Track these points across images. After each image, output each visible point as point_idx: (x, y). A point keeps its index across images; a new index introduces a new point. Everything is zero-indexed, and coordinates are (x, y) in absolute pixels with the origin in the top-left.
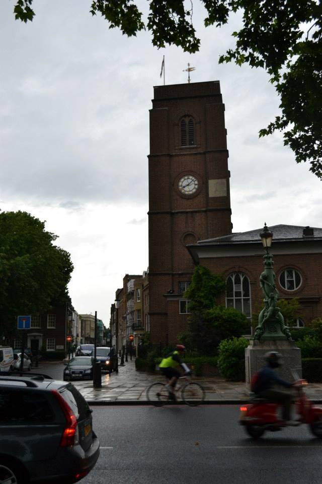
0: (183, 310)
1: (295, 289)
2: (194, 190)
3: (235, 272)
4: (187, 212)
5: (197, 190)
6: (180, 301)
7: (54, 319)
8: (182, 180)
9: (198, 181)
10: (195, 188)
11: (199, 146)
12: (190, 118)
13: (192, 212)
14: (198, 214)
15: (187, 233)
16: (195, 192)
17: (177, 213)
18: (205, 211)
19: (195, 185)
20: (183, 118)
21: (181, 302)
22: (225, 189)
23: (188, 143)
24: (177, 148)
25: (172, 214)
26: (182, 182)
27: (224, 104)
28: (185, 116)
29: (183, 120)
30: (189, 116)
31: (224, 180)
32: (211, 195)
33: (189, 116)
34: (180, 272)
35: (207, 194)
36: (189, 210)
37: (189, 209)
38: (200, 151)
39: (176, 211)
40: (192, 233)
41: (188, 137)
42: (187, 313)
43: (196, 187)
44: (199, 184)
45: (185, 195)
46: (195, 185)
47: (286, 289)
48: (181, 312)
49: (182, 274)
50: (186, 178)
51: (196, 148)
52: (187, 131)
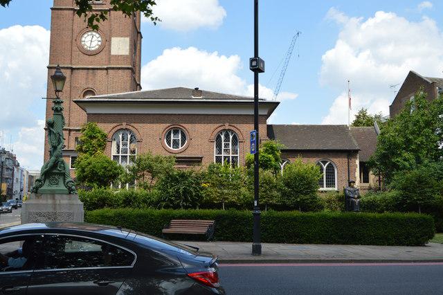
1: (180, 148)
3: (122, 129)
4: (88, 69)
5: (100, 46)
8: (86, 35)
14: (99, 71)
17: (78, 69)
18: (107, 69)
25: (72, 69)
32: (112, 53)
35: (110, 51)
36: (90, 67)
43: (100, 43)
45: (88, 51)
47: (171, 148)
50: (89, 33)
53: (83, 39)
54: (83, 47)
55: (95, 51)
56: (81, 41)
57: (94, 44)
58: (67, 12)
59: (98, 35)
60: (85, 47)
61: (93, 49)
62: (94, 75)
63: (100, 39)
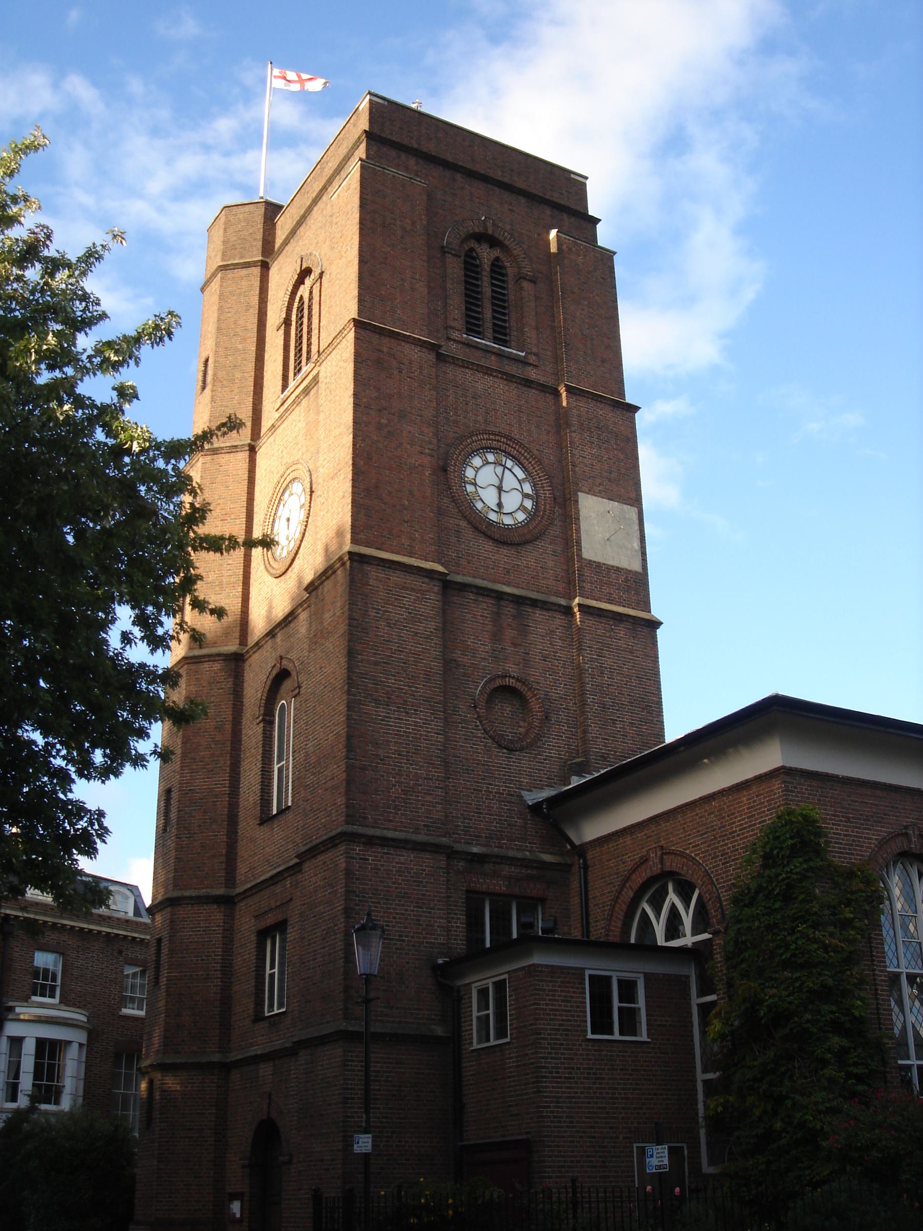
0: (602, 1023)
2: (521, 516)
5: (532, 516)
6: (587, 973)
7: (142, 986)
8: (477, 461)
9: (534, 486)
10: (522, 508)
11: (532, 359)
12: (497, 253)
13: (519, 601)
14: (538, 614)
15: (499, 682)
16: (525, 525)
17: (464, 587)
19: (526, 496)
20: (473, 244)
21: (590, 976)
22: (636, 545)
23: (489, 333)
24: (455, 335)
26: (477, 470)
27: (607, 257)
28: (480, 237)
29: (472, 250)
30: (493, 242)
31: (632, 512)
33: (493, 242)
34: (475, 850)
37: (508, 584)
38: (533, 374)
39: (459, 578)
40: (518, 686)
41: (488, 314)
42: (617, 1036)
44: (536, 498)
45: (490, 523)
46: (526, 496)
48: (593, 1033)
49: (481, 859)
51: (523, 362)
52: (487, 290)
53: (470, 473)
54: (472, 507)
55: (508, 528)
56: (463, 480)
57: (512, 501)
58: (415, 354)
59: (521, 475)
60: (479, 505)
61: (508, 521)
62: (523, 630)
63: (528, 489)
